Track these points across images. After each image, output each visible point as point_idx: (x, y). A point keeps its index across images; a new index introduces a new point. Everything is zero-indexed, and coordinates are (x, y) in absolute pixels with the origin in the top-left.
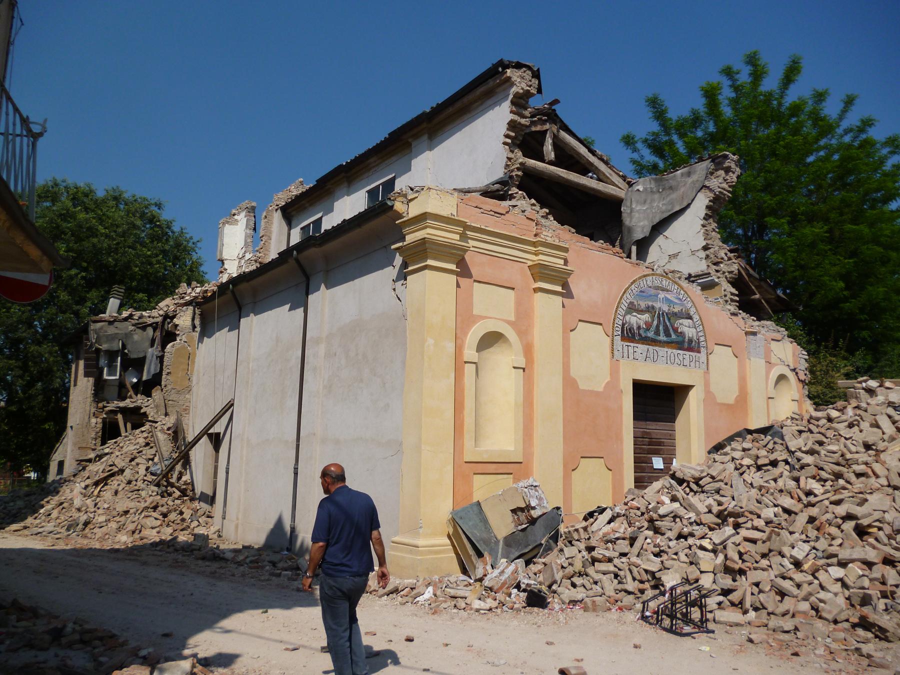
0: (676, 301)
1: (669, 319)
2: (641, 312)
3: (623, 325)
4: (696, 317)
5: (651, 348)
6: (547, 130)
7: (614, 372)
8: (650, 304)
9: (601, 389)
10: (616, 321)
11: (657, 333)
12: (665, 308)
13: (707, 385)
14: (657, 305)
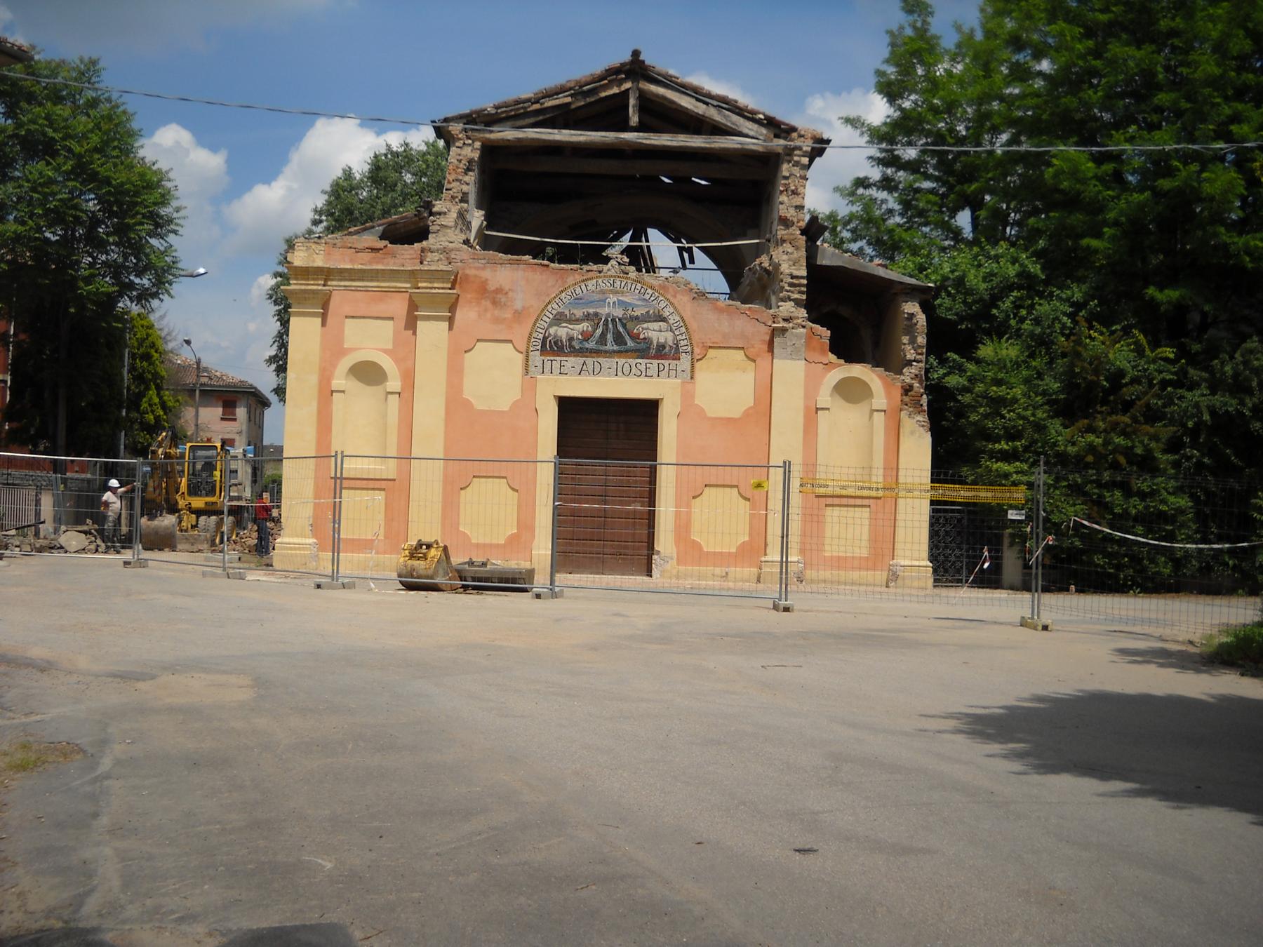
1: (624, 326)
2: (574, 321)
3: (545, 339)
4: (673, 319)
5: (589, 361)
6: (627, 90)
7: (529, 387)
8: (591, 311)
9: (506, 409)
10: (535, 335)
12: (618, 313)
13: (687, 396)
14: (604, 311)
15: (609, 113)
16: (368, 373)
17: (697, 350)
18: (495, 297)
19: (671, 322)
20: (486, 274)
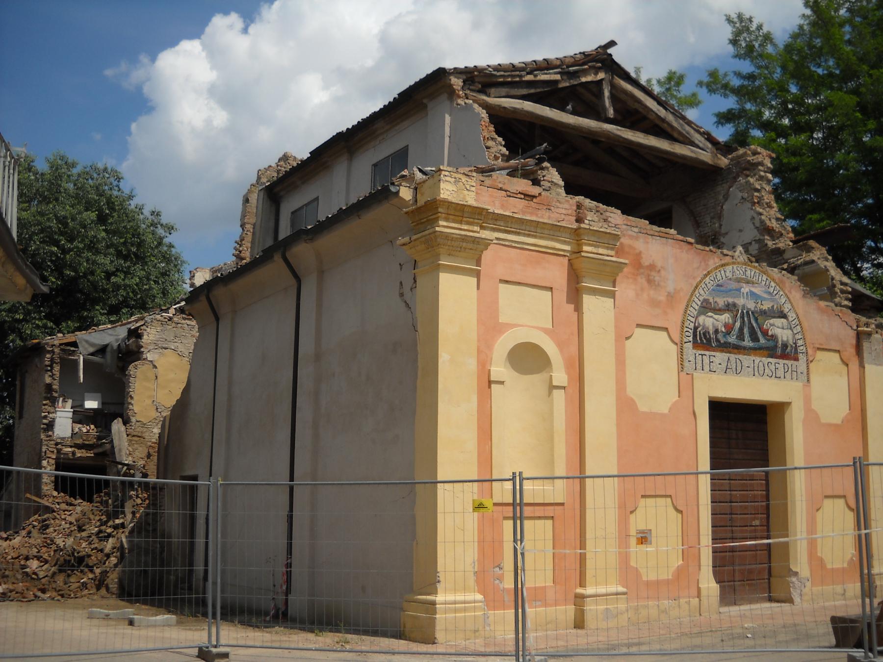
0: (765, 296)
1: (756, 320)
2: (718, 311)
3: (696, 328)
4: (792, 316)
5: (733, 357)
6: (602, 80)
7: (685, 388)
8: (731, 300)
9: (666, 411)
10: (686, 324)
11: (741, 336)
12: (751, 305)
13: (807, 400)
14: (740, 302)
15: (584, 99)
16: (528, 358)
17: (810, 352)
18: (647, 272)
19: (790, 319)
20: (640, 245)
